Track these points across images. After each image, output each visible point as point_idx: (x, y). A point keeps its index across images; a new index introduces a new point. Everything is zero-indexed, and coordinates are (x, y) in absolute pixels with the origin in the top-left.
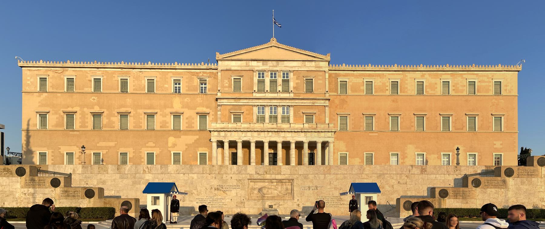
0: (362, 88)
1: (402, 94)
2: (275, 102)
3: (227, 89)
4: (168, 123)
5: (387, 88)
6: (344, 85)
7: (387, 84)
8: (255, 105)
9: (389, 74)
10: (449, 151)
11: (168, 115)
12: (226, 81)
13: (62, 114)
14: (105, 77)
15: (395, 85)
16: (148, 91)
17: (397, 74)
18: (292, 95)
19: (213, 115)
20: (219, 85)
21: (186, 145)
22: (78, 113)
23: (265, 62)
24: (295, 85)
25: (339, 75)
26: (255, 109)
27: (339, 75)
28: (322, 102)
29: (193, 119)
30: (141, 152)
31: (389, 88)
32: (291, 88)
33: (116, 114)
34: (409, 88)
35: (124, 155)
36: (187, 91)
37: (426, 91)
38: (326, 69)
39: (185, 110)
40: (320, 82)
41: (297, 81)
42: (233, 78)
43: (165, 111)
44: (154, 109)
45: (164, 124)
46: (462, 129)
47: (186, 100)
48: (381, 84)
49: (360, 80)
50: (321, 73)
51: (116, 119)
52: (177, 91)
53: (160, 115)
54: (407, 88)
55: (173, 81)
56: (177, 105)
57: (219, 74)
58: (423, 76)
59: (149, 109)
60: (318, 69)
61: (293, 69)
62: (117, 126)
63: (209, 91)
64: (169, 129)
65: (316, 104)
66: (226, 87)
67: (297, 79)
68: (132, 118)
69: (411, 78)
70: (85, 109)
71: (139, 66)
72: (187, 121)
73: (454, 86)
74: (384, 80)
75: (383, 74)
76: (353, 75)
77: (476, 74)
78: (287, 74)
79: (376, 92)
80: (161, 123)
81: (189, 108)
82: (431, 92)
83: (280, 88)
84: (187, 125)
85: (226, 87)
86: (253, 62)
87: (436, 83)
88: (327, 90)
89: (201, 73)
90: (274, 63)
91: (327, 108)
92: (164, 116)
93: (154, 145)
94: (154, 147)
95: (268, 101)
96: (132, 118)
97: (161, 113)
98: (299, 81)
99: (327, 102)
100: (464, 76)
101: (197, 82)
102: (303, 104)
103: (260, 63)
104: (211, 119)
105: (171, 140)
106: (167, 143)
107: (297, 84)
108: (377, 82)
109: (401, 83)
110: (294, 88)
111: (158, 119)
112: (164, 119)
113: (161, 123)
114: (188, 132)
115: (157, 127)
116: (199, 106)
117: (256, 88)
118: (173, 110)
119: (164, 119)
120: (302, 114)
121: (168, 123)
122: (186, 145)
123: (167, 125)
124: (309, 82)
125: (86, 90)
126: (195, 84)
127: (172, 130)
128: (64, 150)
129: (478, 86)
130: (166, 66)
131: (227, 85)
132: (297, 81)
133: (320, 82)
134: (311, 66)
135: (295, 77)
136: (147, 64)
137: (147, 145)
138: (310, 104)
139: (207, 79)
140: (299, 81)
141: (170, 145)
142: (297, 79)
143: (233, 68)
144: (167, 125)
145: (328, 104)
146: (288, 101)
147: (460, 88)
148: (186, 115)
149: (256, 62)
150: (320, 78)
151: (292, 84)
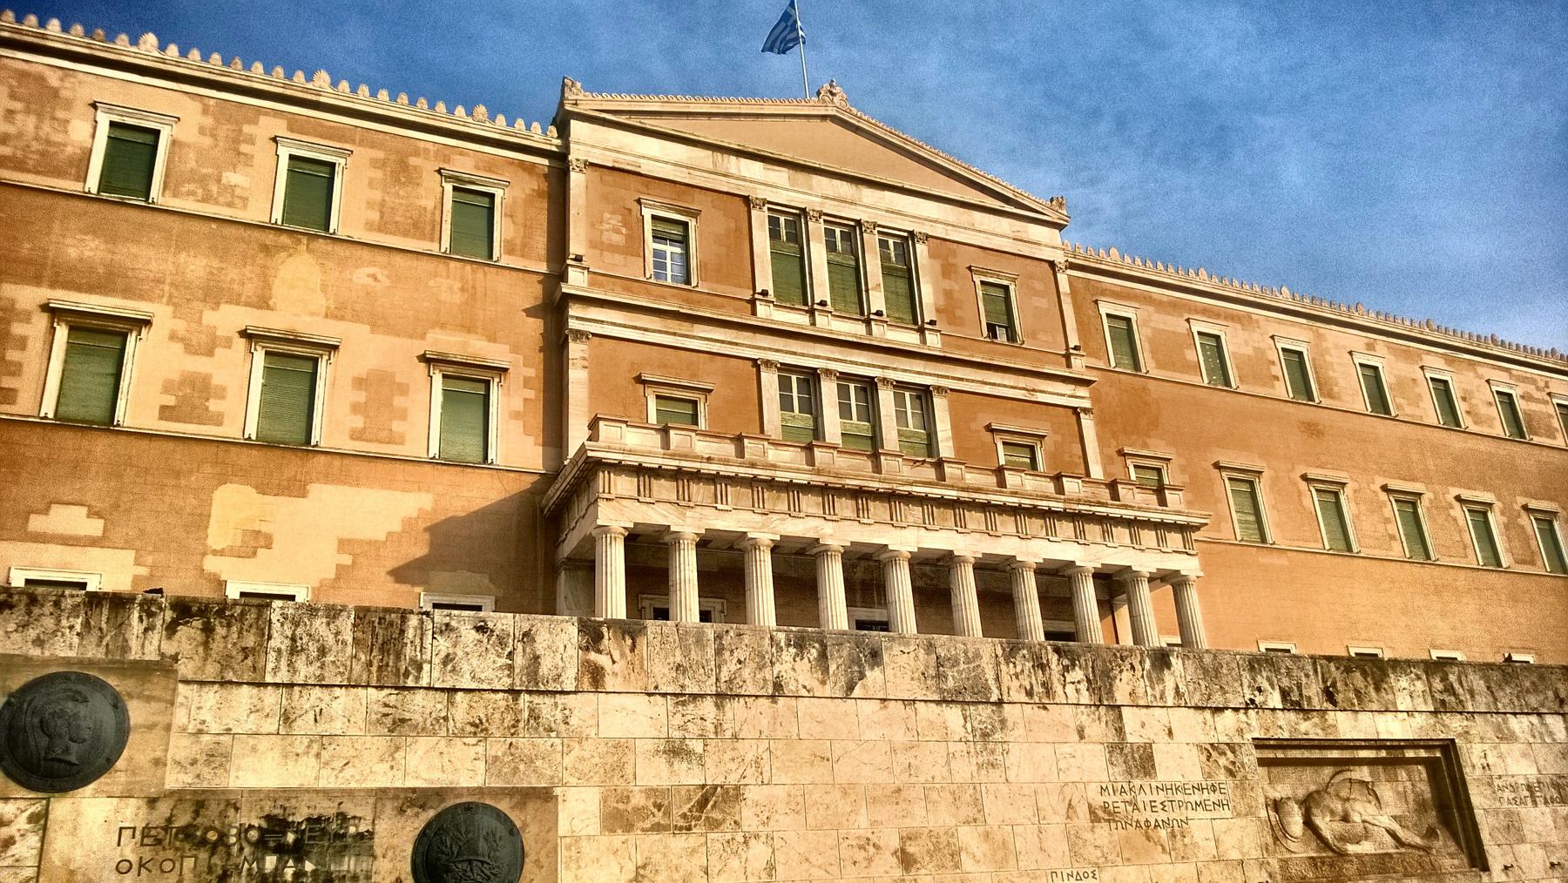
0: (1190, 355)
1: (1326, 402)
2: (862, 364)
3: (618, 258)
4: (221, 393)
5: (1276, 370)
6: (1124, 330)
7: (1273, 356)
8: (768, 363)
11: (228, 343)
12: (615, 221)
16: (104, 185)
18: (934, 342)
19: (527, 382)
21: (344, 544)
23: (801, 177)
36: (370, 226)
37: (1399, 407)
38: (1059, 258)
42: (647, 213)
43: (210, 317)
44: (128, 292)
45: (192, 396)
49: (1176, 324)
53: (173, 337)
55: (284, 163)
56: (300, 294)
58: (1370, 346)
59: (91, 289)
63: (510, 250)
64: (230, 431)
66: (613, 248)
71: (76, 39)
72: (361, 397)
73: (1464, 399)
76: (1147, 299)
77: (1507, 370)
80: (167, 388)
81: (379, 323)
82: (1409, 412)
83: (877, 301)
84: (358, 422)
85: (613, 248)
86: (743, 161)
88: (1074, 341)
89: (466, 160)
90: (844, 189)
93: (95, 527)
94: (93, 542)
95: (836, 352)
97: (181, 326)
99: (1083, 391)
100: (1481, 370)
101: (436, 197)
102: (986, 390)
103: (781, 175)
104: (518, 405)
105: (233, 505)
106: (201, 521)
107: (948, 294)
108: (1235, 343)
110: (938, 311)
111: (149, 368)
112: (199, 365)
113: (167, 388)
114: (368, 464)
116: (443, 326)
117: (765, 281)
118: (274, 321)
119: (199, 365)
121: (221, 393)
122: (344, 544)
123: (214, 405)
127: (247, 444)
129: (1525, 413)
130: (257, 75)
131: (618, 239)
132: (947, 284)
135: (937, 265)
136: (134, 41)
137: (36, 523)
139: (499, 193)
141: (217, 536)
143: (647, 168)
144: (214, 405)
145: (1087, 404)
146: (918, 365)
147: (1484, 410)
149: (758, 165)
150: (1038, 286)
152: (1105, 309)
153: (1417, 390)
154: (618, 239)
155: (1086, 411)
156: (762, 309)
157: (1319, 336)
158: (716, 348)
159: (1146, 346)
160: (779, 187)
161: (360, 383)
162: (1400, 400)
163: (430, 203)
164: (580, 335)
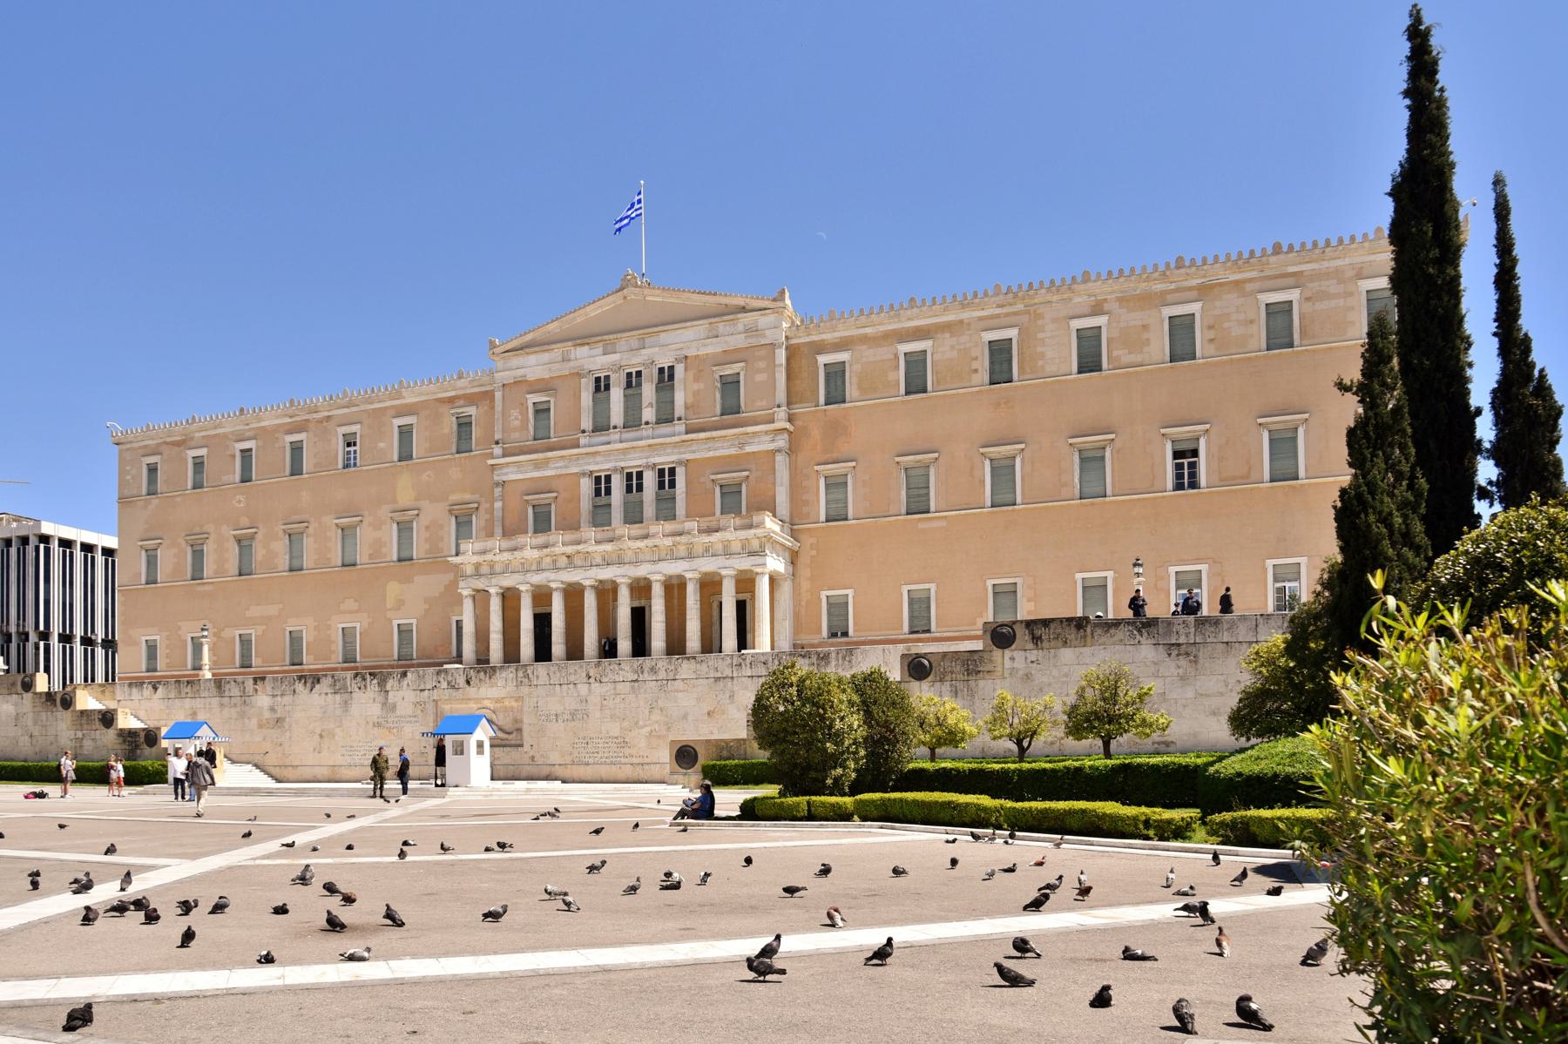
0: (891, 376)
5: (975, 365)
8: (584, 474)
9: (981, 319)
10: (1198, 561)
12: (515, 413)
13: (183, 543)
14: (260, 443)
15: (1000, 353)
17: (1007, 315)
20: (498, 427)
22: (212, 537)
24: (689, 401)
25: (820, 348)
26: (587, 486)
27: (820, 348)
28: (768, 438)
29: (441, 527)
30: (329, 627)
31: (983, 364)
32: (679, 410)
33: (281, 534)
34: (1049, 354)
35: (295, 639)
39: (424, 504)
40: (761, 377)
41: (696, 387)
46: (1248, 476)
47: (424, 477)
48: (955, 353)
50: (763, 352)
51: (281, 546)
52: (406, 456)
54: (1042, 355)
57: (498, 395)
60: (754, 342)
61: (685, 352)
62: (283, 561)
65: (748, 449)
67: (696, 379)
68: (311, 540)
69: (1054, 320)
70: (224, 528)
73: (1210, 327)
74: (963, 339)
75: (961, 322)
78: (671, 368)
79: (937, 382)
87: (1145, 327)
91: (779, 458)
92: (377, 526)
93: (355, 606)
96: (311, 540)
98: (702, 386)
101: (449, 426)
102: (711, 454)
104: (483, 523)
109: (1021, 342)
110: (687, 408)
111: (364, 535)
115: (362, 556)
117: (587, 423)
120: (709, 485)
124: (730, 385)
125: (225, 478)
126: (446, 431)
128: (189, 631)
131: (517, 423)
132: (696, 387)
133: (761, 377)
134: (733, 337)
135: (691, 374)
138: (733, 451)
140: (702, 386)
142: (696, 379)
143: (531, 377)
148: (424, 519)
150: (762, 365)
151: (680, 398)
152: (823, 359)
153: (1145, 336)
154: (517, 423)
155: (779, 451)
156: (583, 441)
157: (1040, 316)
158: (559, 472)
159: (855, 380)
160: (595, 360)
161: (427, 528)
162: (1115, 353)
163: (446, 431)
164: (497, 484)
